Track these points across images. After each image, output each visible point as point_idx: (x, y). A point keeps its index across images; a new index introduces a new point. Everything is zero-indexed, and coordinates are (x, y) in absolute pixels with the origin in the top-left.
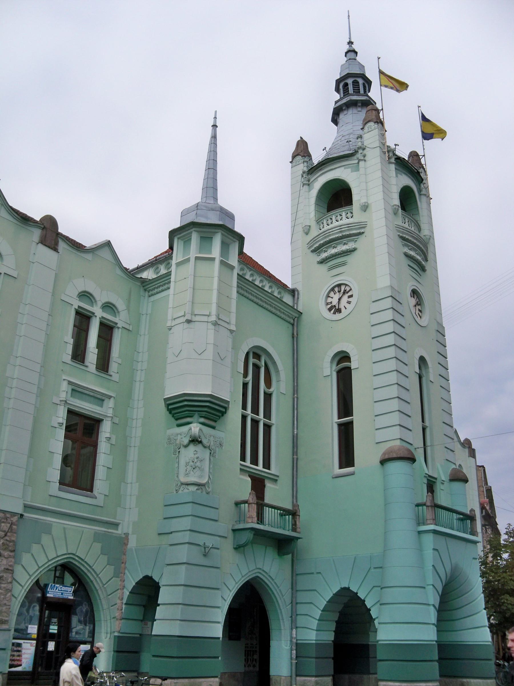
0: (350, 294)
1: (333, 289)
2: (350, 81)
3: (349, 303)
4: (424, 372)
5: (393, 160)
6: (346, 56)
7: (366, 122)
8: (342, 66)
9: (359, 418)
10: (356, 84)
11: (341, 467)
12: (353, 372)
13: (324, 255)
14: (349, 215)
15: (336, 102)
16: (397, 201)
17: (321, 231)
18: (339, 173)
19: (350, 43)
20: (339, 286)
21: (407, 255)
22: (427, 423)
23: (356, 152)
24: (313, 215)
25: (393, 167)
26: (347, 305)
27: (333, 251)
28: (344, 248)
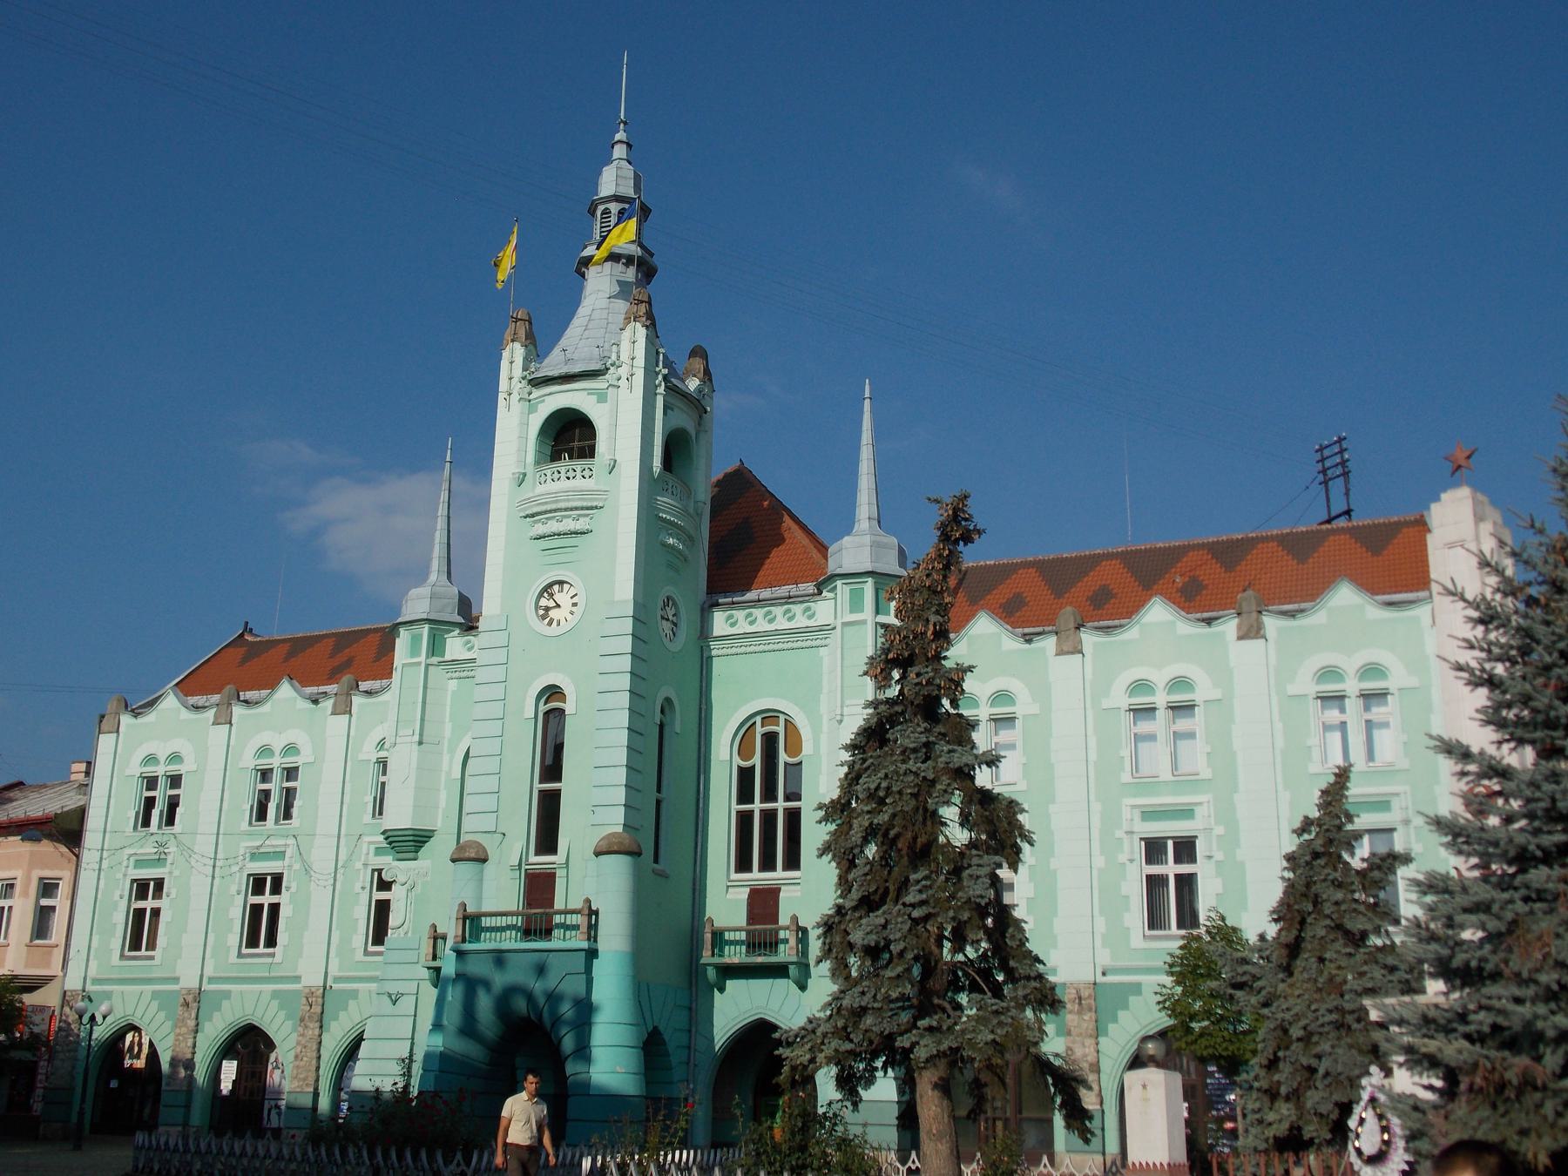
0: (575, 600)
3: (572, 613)
4: (667, 720)
7: (627, 320)
9: (568, 786)
11: (537, 853)
13: (541, 529)
14: (587, 473)
17: (540, 489)
20: (561, 583)
22: (663, 795)
24: (531, 457)
26: (569, 617)
27: (554, 526)
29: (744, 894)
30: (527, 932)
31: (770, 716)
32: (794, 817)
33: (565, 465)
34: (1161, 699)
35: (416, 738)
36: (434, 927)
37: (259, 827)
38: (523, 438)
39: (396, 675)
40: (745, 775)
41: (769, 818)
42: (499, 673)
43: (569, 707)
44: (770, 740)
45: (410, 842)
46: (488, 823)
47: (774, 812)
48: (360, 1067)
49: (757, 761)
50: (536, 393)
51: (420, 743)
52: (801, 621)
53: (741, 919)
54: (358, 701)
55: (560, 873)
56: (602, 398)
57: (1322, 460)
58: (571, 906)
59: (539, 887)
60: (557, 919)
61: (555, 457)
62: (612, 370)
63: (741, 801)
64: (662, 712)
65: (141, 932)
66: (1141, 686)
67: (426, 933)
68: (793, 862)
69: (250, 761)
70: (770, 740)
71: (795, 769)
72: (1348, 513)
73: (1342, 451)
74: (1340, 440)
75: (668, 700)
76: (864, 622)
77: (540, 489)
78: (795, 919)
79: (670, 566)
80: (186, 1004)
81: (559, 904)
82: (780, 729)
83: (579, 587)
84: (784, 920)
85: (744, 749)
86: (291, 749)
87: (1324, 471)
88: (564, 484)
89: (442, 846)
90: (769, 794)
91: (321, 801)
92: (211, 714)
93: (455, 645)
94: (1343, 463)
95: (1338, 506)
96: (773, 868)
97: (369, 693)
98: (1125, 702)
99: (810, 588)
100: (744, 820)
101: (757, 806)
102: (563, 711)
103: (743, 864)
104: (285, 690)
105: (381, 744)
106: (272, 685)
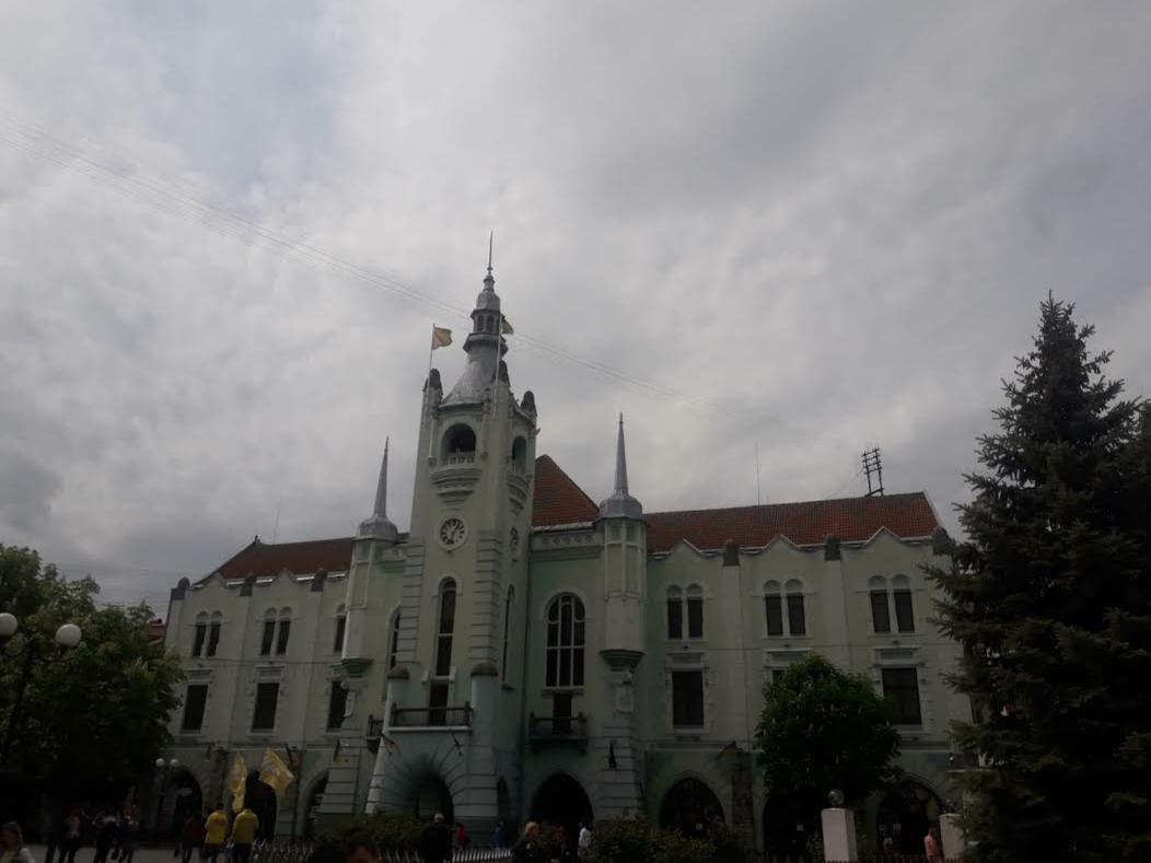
1: (448, 522)
2: (485, 316)
3: (461, 537)
5: (512, 414)
6: (485, 281)
8: (480, 296)
10: (490, 320)
11: (438, 674)
12: (457, 599)
13: (444, 490)
15: (471, 335)
16: (510, 454)
17: (445, 468)
18: (467, 419)
19: (490, 269)
20: (455, 521)
21: (512, 500)
22: (509, 639)
23: (482, 403)
25: (511, 420)
27: (452, 489)
28: (464, 488)
29: (550, 702)
30: (432, 722)
31: (567, 597)
32: (580, 654)
33: (459, 453)
34: (783, 592)
35: (364, 606)
36: (371, 717)
37: (265, 658)
38: (435, 440)
39: (352, 573)
40: (552, 631)
41: (566, 654)
42: (418, 571)
43: (458, 591)
44: (566, 609)
45: (358, 667)
46: (409, 656)
47: (569, 650)
48: (325, 798)
49: (560, 621)
50: (443, 416)
51: (365, 609)
52: (584, 542)
53: (550, 713)
54: (326, 584)
55: (450, 686)
56: (479, 419)
57: (866, 461)
58: (457, 706)
59: (439, 693)
60: (449, 713)
61: (453, 450)
62: (486, 404)
63: (549, 645)
64: (509, 593)
65: (194, 719)
66: (772, 583)
67: (367, 720)
68: (579, 680)
69: (261, 616)
70: (566, 609)
71: (581, 628)
72: (881, 490)
73: (877, 457)
74: (876, 451)
75: (512, 587)
76: (620, 545)
77: (445, 468)
78: (581, 714)
79: (513, 511)
80: (218, 761)
81: (450, 704)
82: (573, 604)
83: (464, 523)
84: (575, 714)
85: (552, 615)
86: (287, 610)
87: (867, 467)
88: (457, 466)
89: (379, 671)
90: (566, 641)
91: (307, 643)
92: (239, 590)
93: (388, 554)
94: (878, 463)
95: (875, 486)
96: (568, 684)
97: (333, 580)
98: (761, 592)
99: (590, 524)
100: (551, 655)
101: (559, 647)
102: (454, 592)
103: (551, 681)
104: (284, 578)
105: (342, 607)
106: (275, 573)
